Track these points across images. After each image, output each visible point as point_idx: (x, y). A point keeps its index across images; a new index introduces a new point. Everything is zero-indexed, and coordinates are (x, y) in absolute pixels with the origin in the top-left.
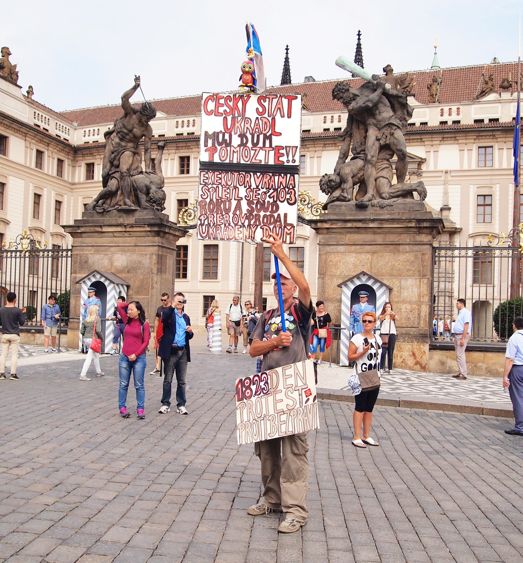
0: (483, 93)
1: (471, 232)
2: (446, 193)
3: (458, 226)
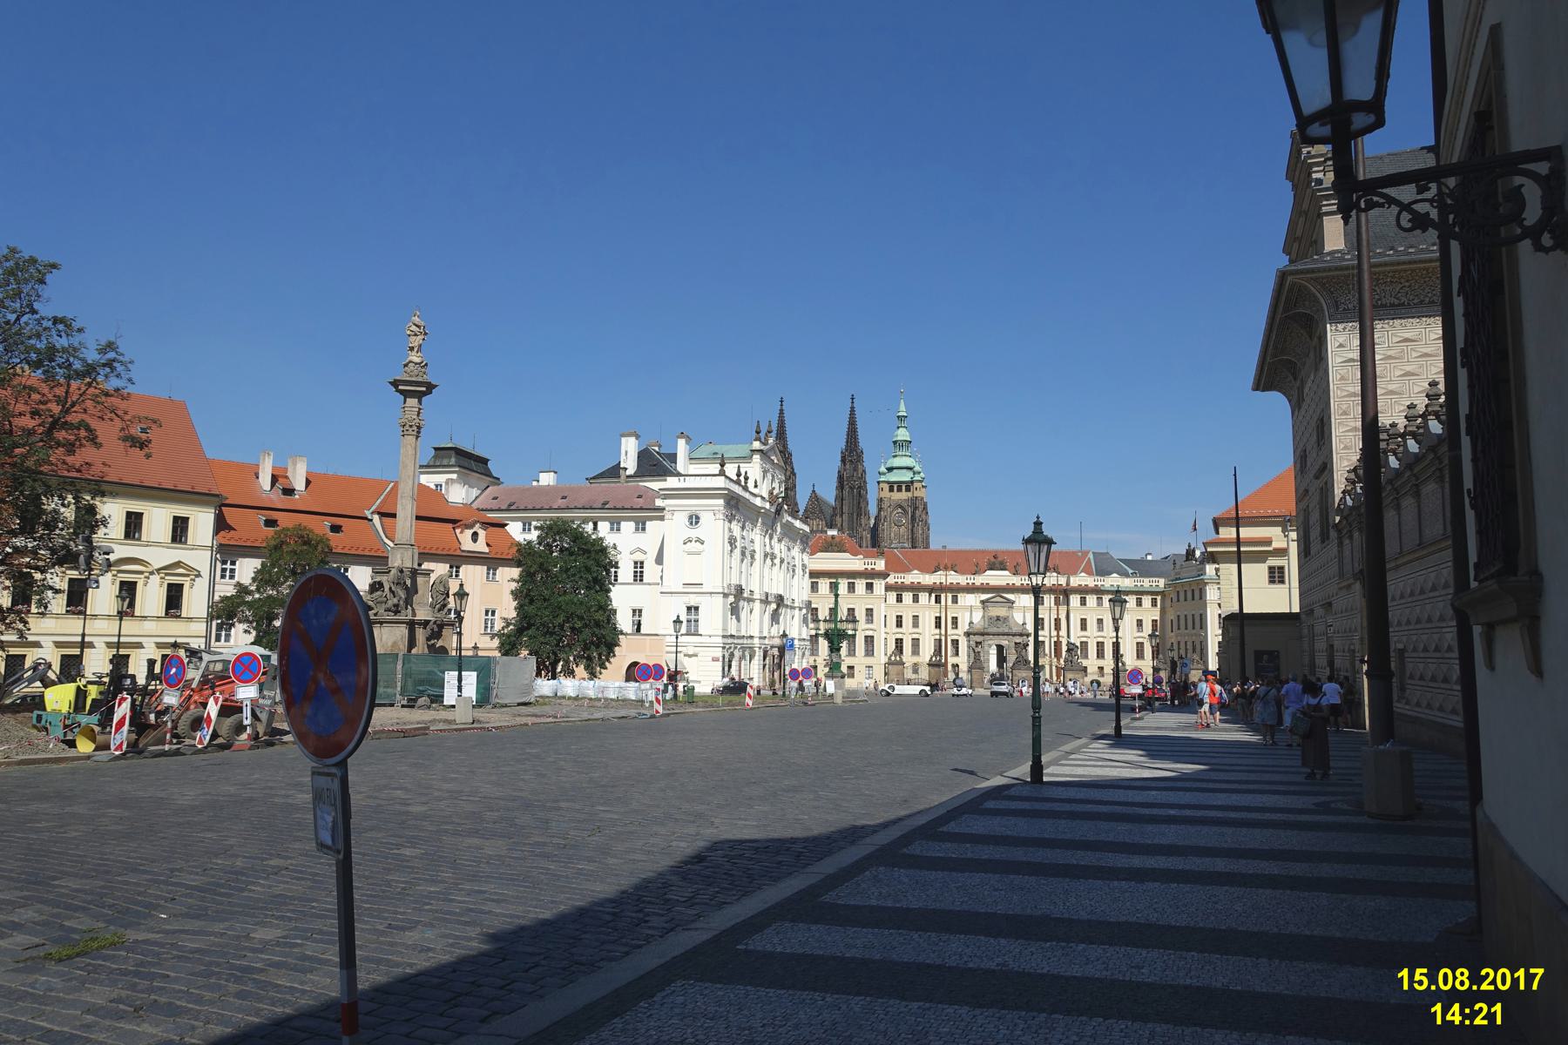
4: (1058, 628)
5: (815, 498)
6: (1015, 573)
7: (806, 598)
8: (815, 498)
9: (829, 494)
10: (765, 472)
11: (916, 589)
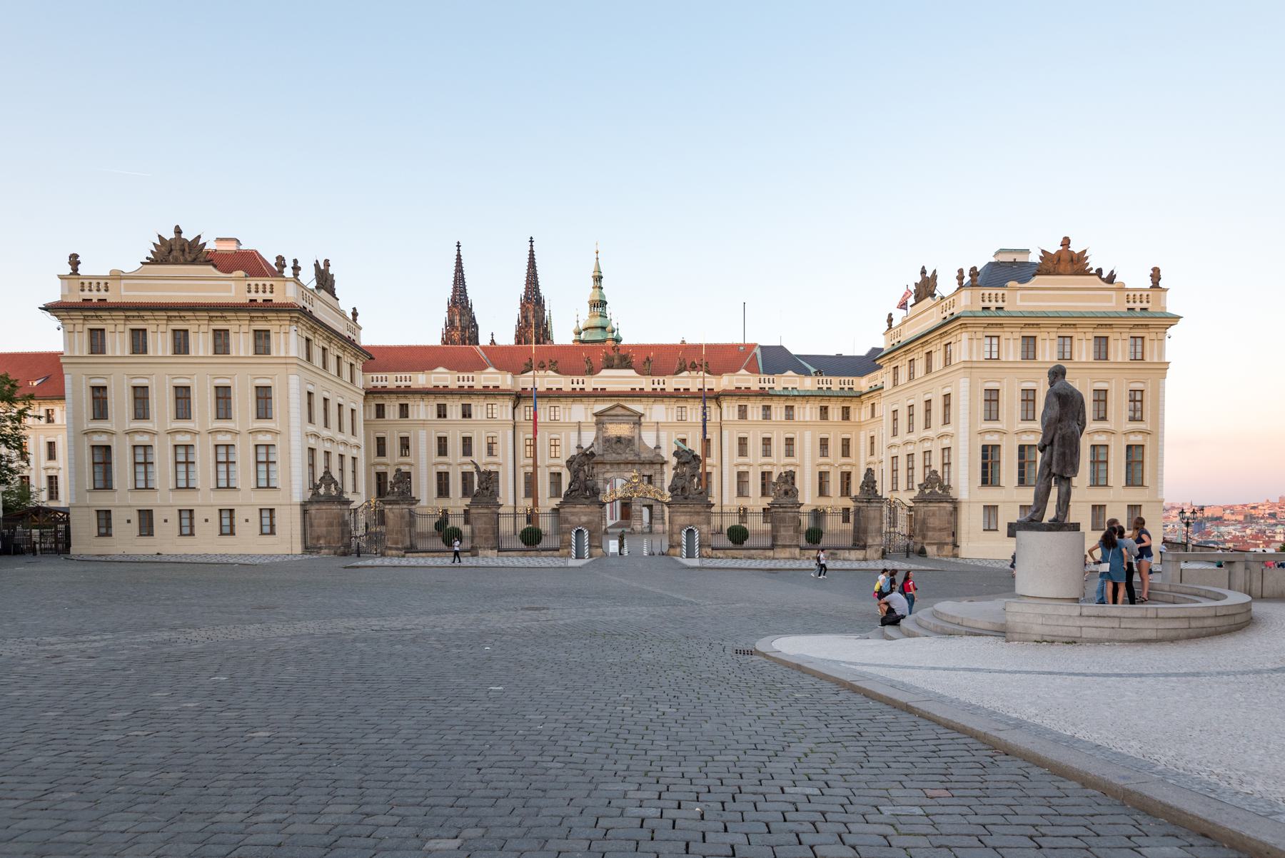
0: (680, 371)
2: (658, 437)
6: (641, 373)
11: (491, 393)
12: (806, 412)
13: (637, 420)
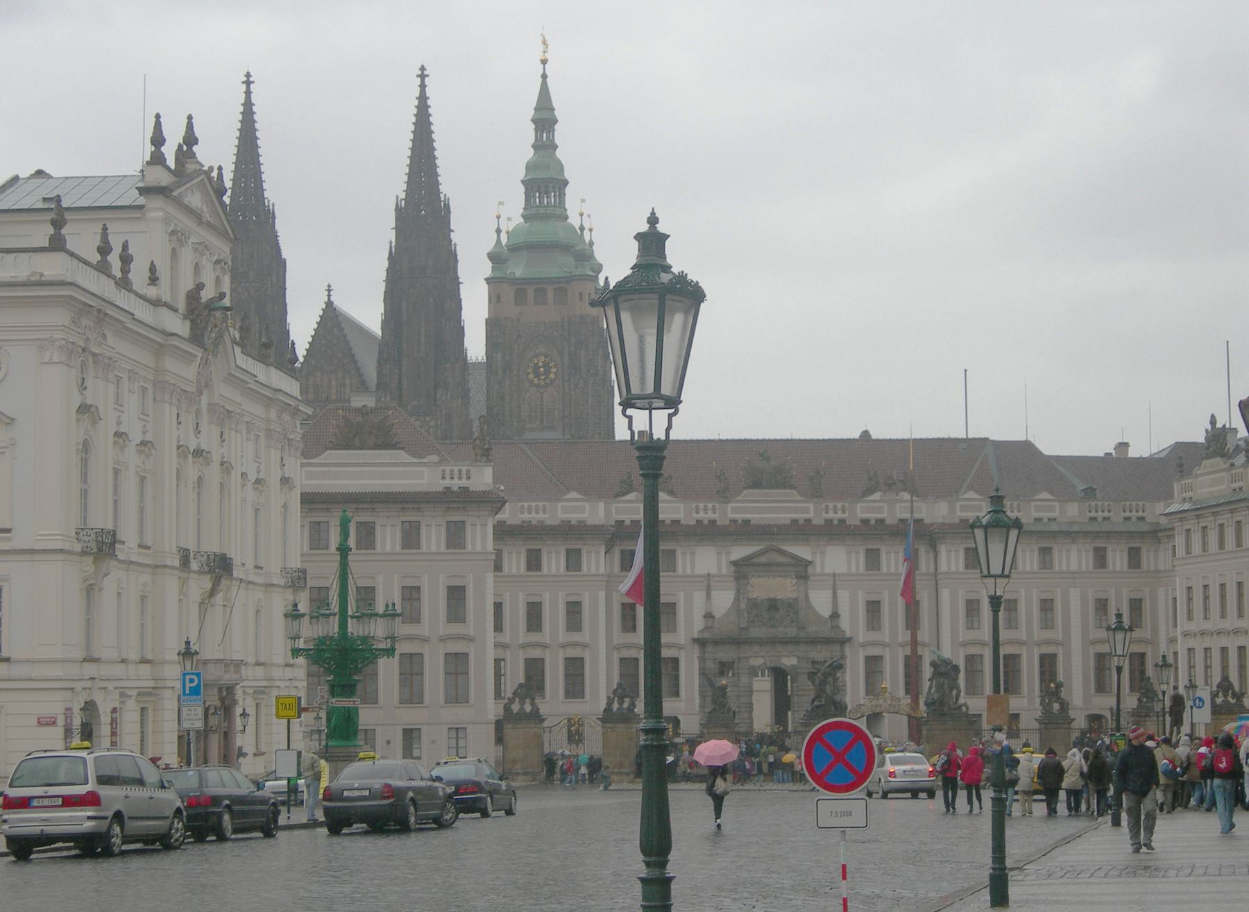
0: (870, 491)
1: (861, 640)
3: (848, 635)
4: (912, 621)
5: (332, 322)
6: (816, 492)
7: (295, 562)
8: (332, 320)
9: (368, 311)
10: (178, 236)
11: (573, 534)
12: (1073, 558)
13: (802, 570)
